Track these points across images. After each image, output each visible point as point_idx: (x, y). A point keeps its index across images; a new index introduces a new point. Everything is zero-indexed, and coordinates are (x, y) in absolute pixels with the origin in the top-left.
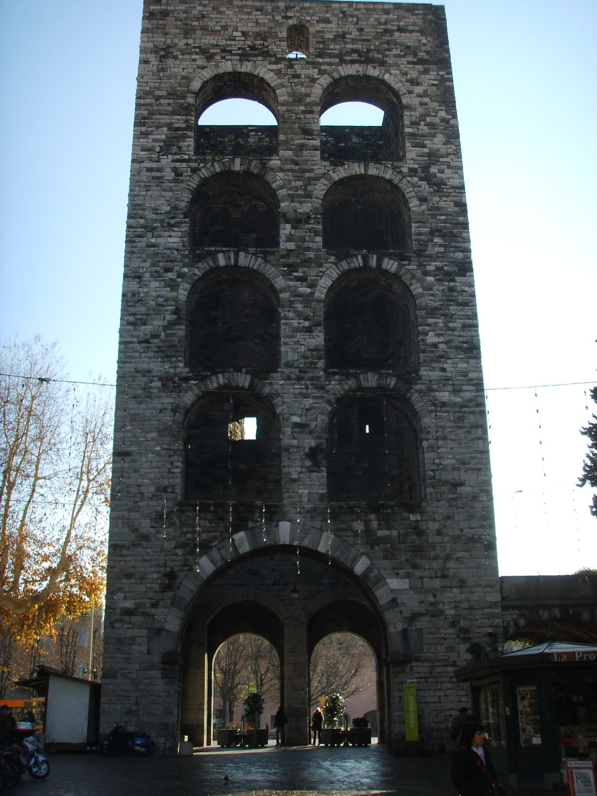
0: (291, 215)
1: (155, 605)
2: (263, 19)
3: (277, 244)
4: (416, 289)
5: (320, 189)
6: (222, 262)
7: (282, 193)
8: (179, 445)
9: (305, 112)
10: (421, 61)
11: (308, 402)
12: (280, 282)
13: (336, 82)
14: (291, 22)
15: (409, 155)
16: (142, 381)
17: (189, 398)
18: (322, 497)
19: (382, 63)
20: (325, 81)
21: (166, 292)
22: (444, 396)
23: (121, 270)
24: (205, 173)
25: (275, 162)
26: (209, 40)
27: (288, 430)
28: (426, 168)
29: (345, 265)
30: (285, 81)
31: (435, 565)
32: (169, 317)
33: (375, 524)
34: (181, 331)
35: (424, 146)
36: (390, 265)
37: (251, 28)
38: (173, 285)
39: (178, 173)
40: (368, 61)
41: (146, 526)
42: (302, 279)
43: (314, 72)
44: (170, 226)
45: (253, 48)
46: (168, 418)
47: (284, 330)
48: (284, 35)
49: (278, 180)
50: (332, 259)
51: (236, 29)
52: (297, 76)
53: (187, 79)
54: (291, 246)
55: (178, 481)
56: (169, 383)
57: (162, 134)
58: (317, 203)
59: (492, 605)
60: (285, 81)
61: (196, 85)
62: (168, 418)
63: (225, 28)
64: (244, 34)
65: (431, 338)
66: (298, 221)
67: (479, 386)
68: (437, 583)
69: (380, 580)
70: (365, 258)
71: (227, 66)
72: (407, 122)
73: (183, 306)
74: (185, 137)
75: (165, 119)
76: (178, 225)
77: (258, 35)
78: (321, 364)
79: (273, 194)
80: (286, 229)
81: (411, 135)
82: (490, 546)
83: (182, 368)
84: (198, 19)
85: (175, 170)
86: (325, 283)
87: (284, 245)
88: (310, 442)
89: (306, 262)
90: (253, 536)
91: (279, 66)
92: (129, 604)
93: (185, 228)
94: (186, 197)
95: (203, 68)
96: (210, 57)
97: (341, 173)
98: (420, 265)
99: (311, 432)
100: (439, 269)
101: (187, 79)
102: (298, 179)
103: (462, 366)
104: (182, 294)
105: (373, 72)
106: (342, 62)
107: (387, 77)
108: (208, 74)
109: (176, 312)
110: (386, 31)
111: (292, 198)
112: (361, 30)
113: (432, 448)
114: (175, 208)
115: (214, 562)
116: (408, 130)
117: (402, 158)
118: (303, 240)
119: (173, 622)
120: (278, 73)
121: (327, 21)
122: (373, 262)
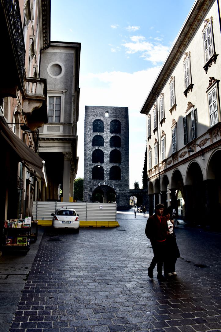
0: (106, 142)
1: (89, 192)
2: (102, 110)
3: (104, 146)
4: (121, 152)
5: (109, 138)
6: (97, 149)
7: (104, 138)
8: (92, 173)
9: (108, 126)
10: (124, 117)
11: (107, 168)
12: (104, 151)
13: (112, 121)
14: (106, 110)
15: (122, 132)
16: (87, 165)
17: (93, 167)
18: (109, 179)
19: (119, 117)
20: (111, 120)
21: (89, 153)
22: (124, 167)
23: (84, 149)
24: (94, 135)
25: (103, 134)
26: (95, 114)
27: (105, 171)
28: (124, 134)
29: (112, 149)
30: (105, 121)
31: (122, 188)
32: (90, 156)
33: (115, 183)
34: (92, 158)
35: (124, 131)
36: (118, 149)
37: (100, 111)
38: (90, 152)
39: (91, 135)
40: (117, 117)
41: (88, 183)
42: (107, 151)
43: (109, 119)
44: (90, 143)
45: (101, 115)
46: (90, 169)
47: (104, 158)
48: (105, 112)
49: (104, 136)
50: (111, 148)
51: (98, 112)
52: (107, 120)
53: (91, 120)
54: (106, 146)
55: (92, 177)
56: (90, 165)
57: (88, 129)
58: (109, 140)
59: (129, 192)
60: (105, 121)
61: (93, 121)
62: (90, 169)
63: (96, 111)
64: (99, 112)
65: (123, 159)
66: (107, 143)
67: (129, 166)
68: (122, 190)
69: (115, 189)
70: (115, 148)
71: (97, 118)
72: (122, 127)
73: (92, 154)
74: (91, 130)
75: (88, 127)
76: (91, 143)
77: (101, 112)
78: (109, 162)
79: (103, 138)
80: (105, 144)
81: (122, 129)
82: (129, 186)
83: (92, 163)
84: (93, 110)
85: (90, 135)
86: (110, 151)
87: (105, 146)
88: (107, 173)
89: (107, 149)
90: (100, 184)
91: (105, 118)
92: (86, 192)
93: (92, 143)
94: (92, 139)
95: (94, 118)
96: (94, 116)
97: (112, 135)
98: (122, 149)
99: (108, 171)
100: (125, 149)
101: (91, 120)
102: (106, 136)
103: (127, 163)
104: (92, 153)
105: (118, 119)
106: (113, 117)
107: (120, 120)
108: (94, 119)
109: (91, 155)
110: (119, 112)
111: (106, 139)
112: (116, 112)
113: (122, 173)
114: (90, 141)
115: (96, 187)
116: (122, 128)
117: (121, 133)
118: (107, 145)
119: (91, 194)
120: (104, 119)
121: (111, 110)
122: (116, 149)
